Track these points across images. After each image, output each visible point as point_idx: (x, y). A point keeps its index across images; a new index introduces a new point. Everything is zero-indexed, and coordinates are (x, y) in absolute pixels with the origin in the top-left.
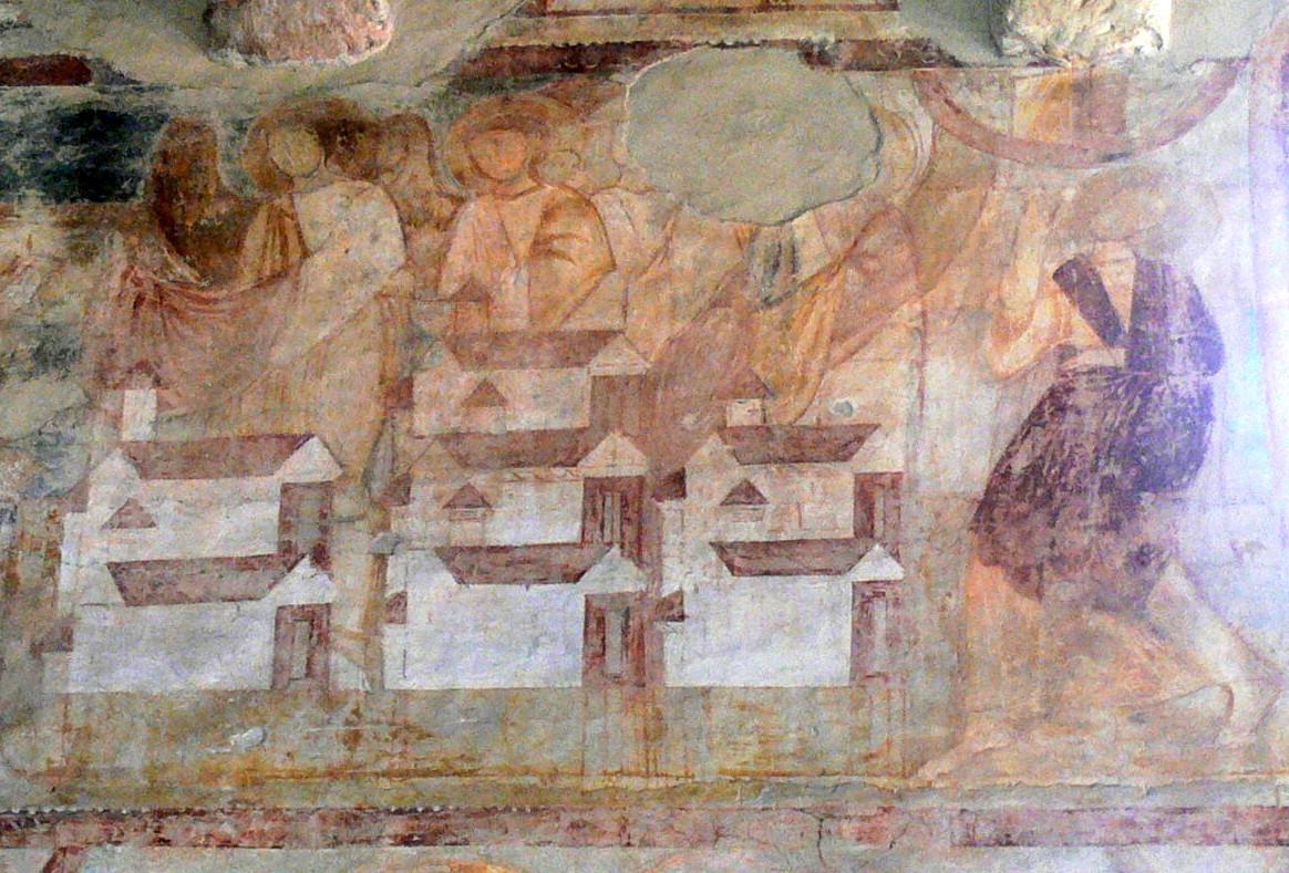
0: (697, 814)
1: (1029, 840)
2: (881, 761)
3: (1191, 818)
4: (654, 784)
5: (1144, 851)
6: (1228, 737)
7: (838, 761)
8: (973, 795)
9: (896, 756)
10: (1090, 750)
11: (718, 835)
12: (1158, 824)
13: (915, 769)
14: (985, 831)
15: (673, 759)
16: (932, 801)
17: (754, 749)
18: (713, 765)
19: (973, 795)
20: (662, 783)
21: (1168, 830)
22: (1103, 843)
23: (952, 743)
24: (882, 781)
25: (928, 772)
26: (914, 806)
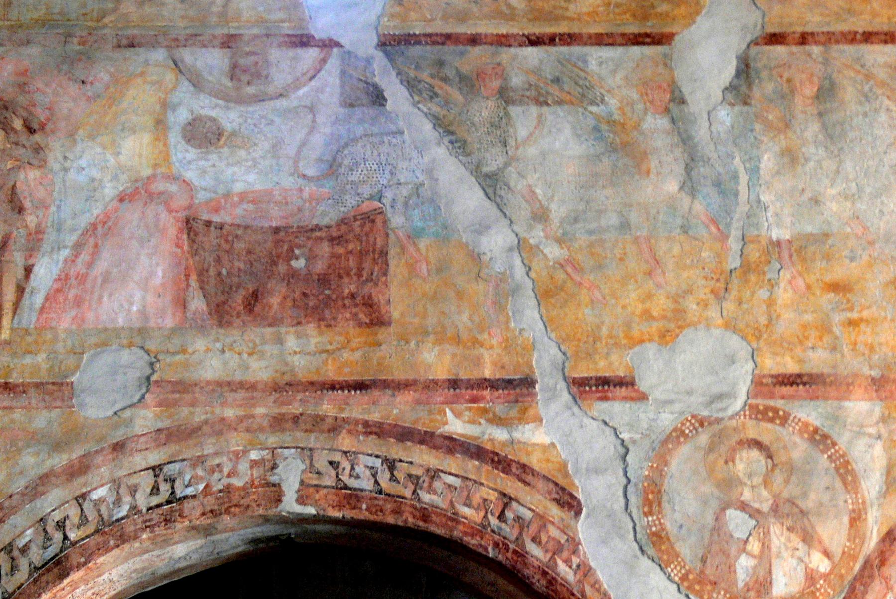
0: (22, 34)
1: (140, 45)
2: (89, 17)
3: (198, 38)
4: (6, 23)
5: (181, 49)
6: (214, 9)
7: (75, 15)
8: (120, 29)
9: (95, 14)
10: (165, 13)
11: (28, 42)
12: (186, 40)
13: (102, 18)
14: (125, 42)
15: (14, 15)
16: (106, 31)
17: (44, 11)
18: (29, 16)
19: (120, 29)
20: (9, 23)
21: (190, 42)
22: (167, 47)
23: (115, 10)
24: (89, 24)
25: (106, 21)
26: (100, 32)
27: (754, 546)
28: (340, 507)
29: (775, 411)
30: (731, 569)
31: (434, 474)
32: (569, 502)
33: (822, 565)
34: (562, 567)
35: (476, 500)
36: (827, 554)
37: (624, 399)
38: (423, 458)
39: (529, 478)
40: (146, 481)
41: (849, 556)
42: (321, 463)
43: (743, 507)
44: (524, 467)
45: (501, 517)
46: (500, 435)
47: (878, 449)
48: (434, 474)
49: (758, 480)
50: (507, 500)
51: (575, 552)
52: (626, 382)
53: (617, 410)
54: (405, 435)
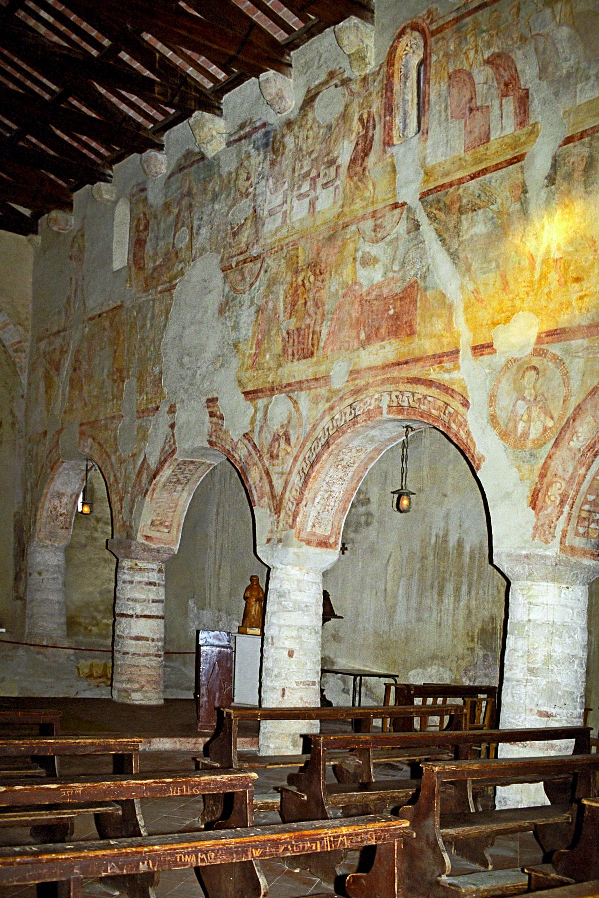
27: (525, 417)
28: (399, 414)
29: (543, 350)
30: (516, 427)
31: (425, 397)
32: (466, 404)
33: (550, 423)
34: (461, 432)
35: (437, 407)
36: (552, 418)
37: (489, 354)
38: (422, 390)
39: (454, 395)
40: (348, 410)
41: (561, 418)
42: (394, 397)
43: (524, 399)
44: (453, 390)
45: (444, 413)
46: (446, 376)
47: (581, 362)
48: (425, 397)
49: (531, 386)
50: (447, 404)
51: (466, 425)
52: (490, 346)
53: (486, 358)
54: (416, 381)
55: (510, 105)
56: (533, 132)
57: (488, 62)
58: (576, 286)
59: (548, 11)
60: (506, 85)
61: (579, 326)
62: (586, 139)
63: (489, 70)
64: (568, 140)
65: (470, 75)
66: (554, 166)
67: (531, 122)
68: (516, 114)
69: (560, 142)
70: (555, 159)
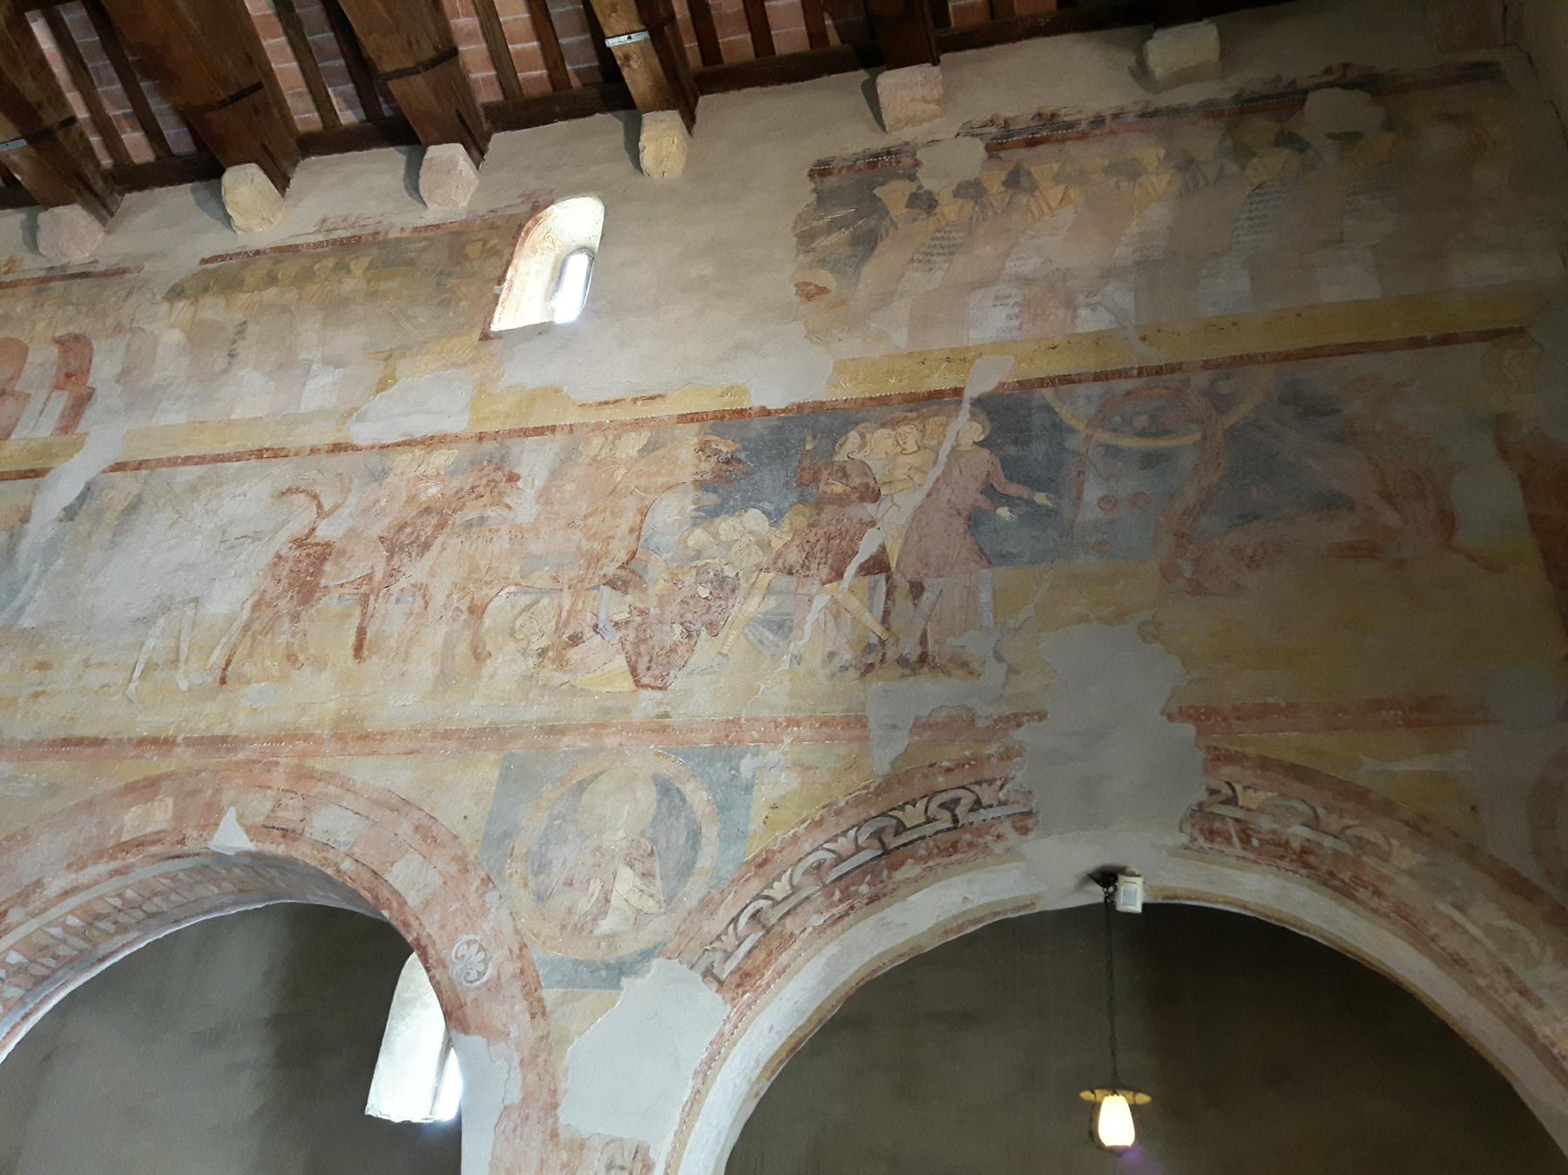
55: (60, 402)
56: (78, 446)
57: (59, 342)
58: (35, 675)
59: (165, 306)
60: (68, 376)
61: (13, 739)
62: (144, 472)
63: (55, 351)
64: (119, 467)
65: (25, 351)
66: (83, 497)
67: (79, 430)
68: (62, 416)
69: (105, 466)
70: (88, 488)
